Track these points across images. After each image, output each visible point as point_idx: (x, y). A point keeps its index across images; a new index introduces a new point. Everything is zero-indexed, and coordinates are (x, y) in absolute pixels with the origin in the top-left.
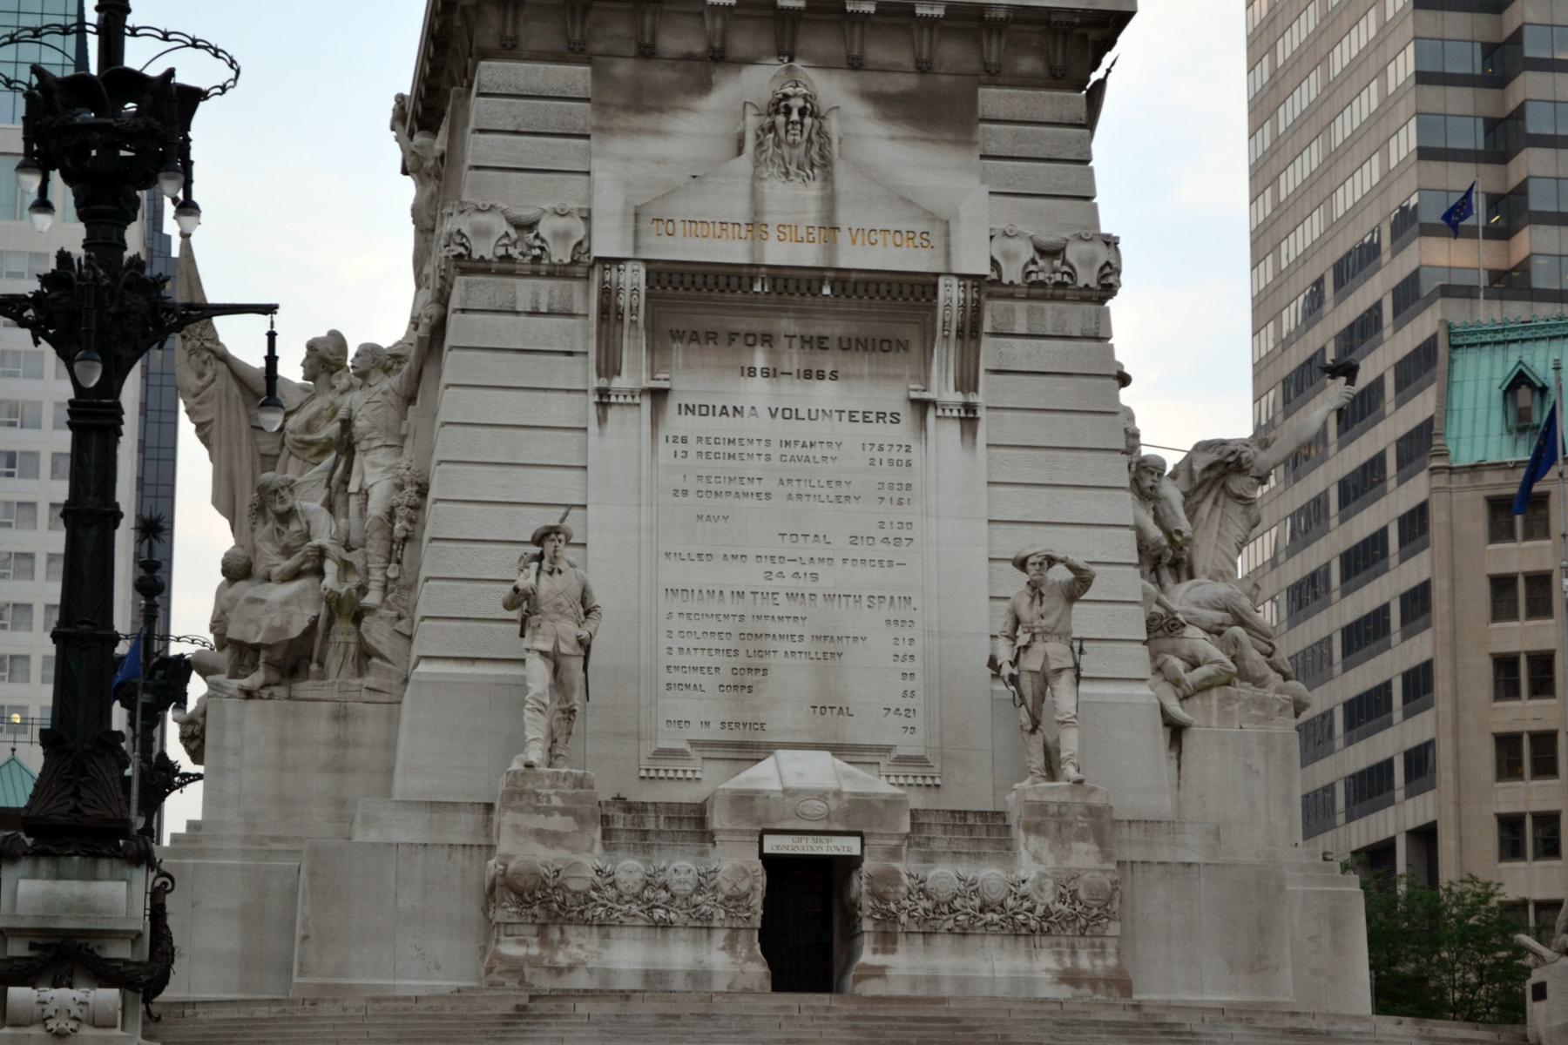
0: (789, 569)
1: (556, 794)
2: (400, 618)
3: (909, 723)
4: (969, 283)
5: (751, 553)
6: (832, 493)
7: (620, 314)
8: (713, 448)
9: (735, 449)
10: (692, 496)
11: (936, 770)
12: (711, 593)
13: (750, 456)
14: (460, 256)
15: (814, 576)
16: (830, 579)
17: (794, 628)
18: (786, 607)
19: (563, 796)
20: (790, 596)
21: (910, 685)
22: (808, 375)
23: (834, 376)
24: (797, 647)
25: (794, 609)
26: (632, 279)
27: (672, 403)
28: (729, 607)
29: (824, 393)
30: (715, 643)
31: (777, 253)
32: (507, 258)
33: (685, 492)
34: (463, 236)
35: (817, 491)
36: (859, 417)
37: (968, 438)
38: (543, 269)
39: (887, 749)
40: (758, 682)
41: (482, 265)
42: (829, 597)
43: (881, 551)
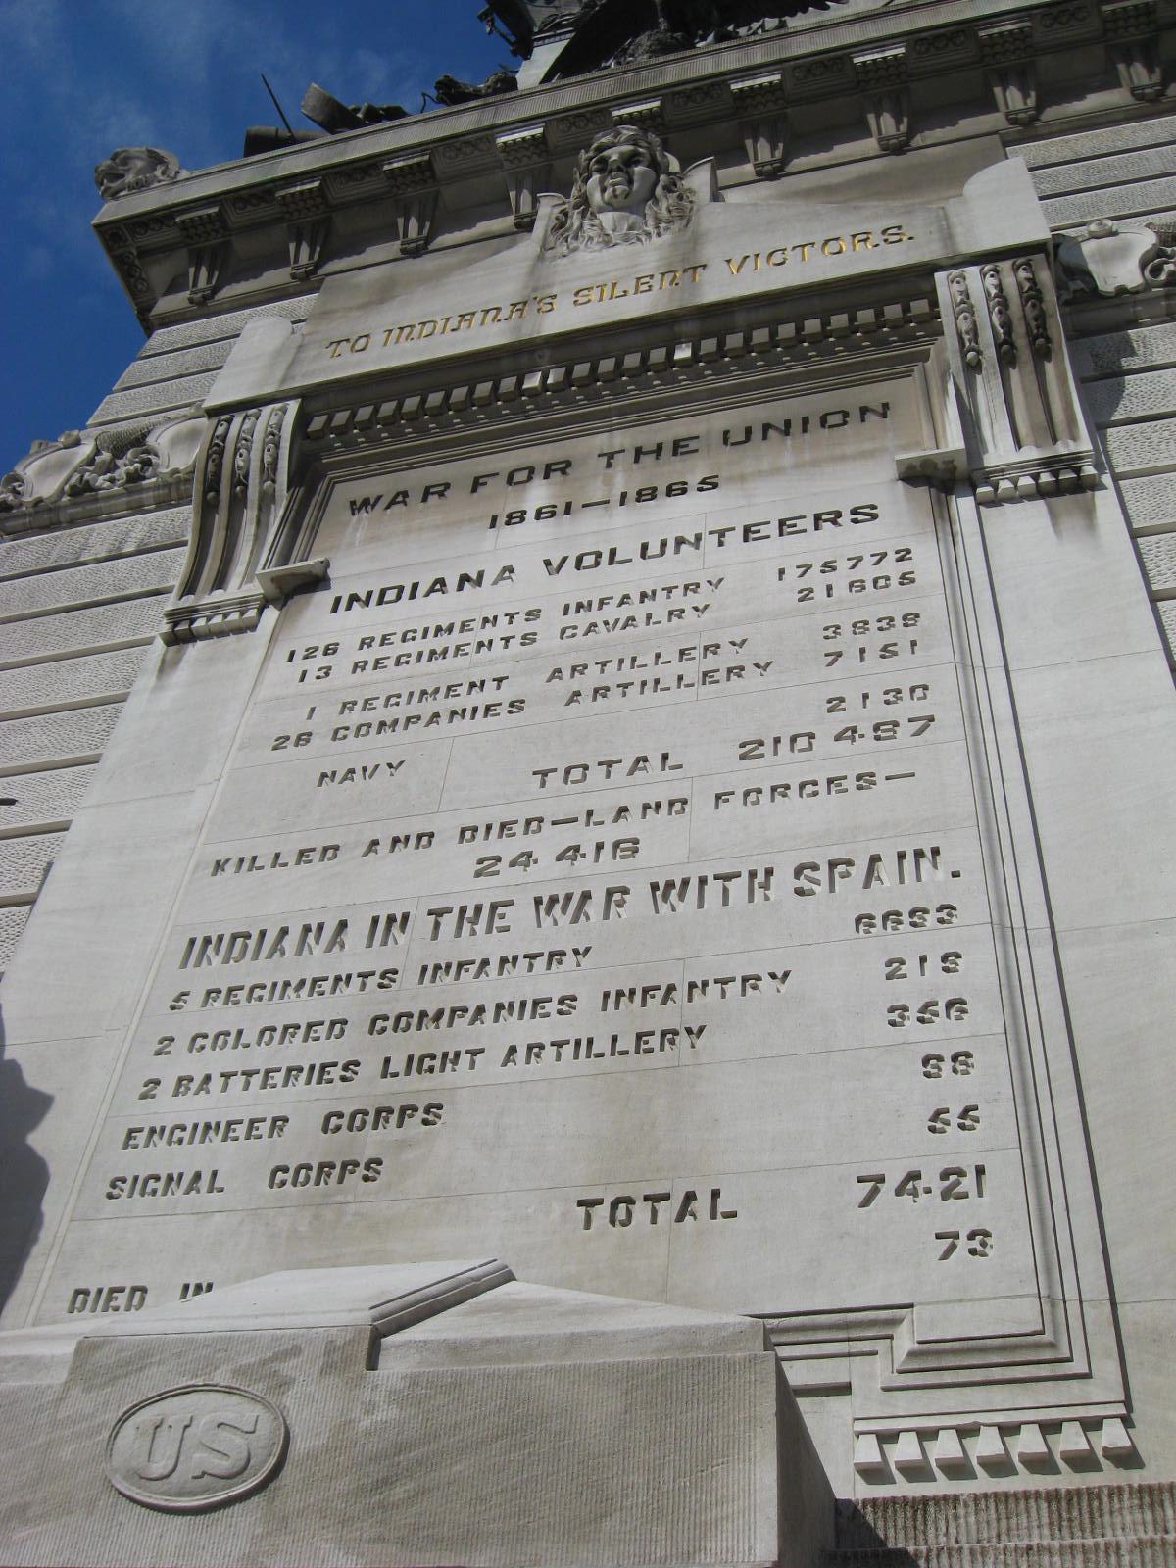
3: (960, 1216)
4: (1005, 266)
6: (691, 670)
11: (1104, 1387)
15: (628, 847)
17: (549, 983)
20: (545, 905)
21: (952, 1091)
23: (709, 484)
24: (541, 1030)
25: (560, 932)
28: (356, 955)
33: (304, 738)
39: (880, 1322)
40: (404, 1144)
42: (663, 891)
43: (832, 758)
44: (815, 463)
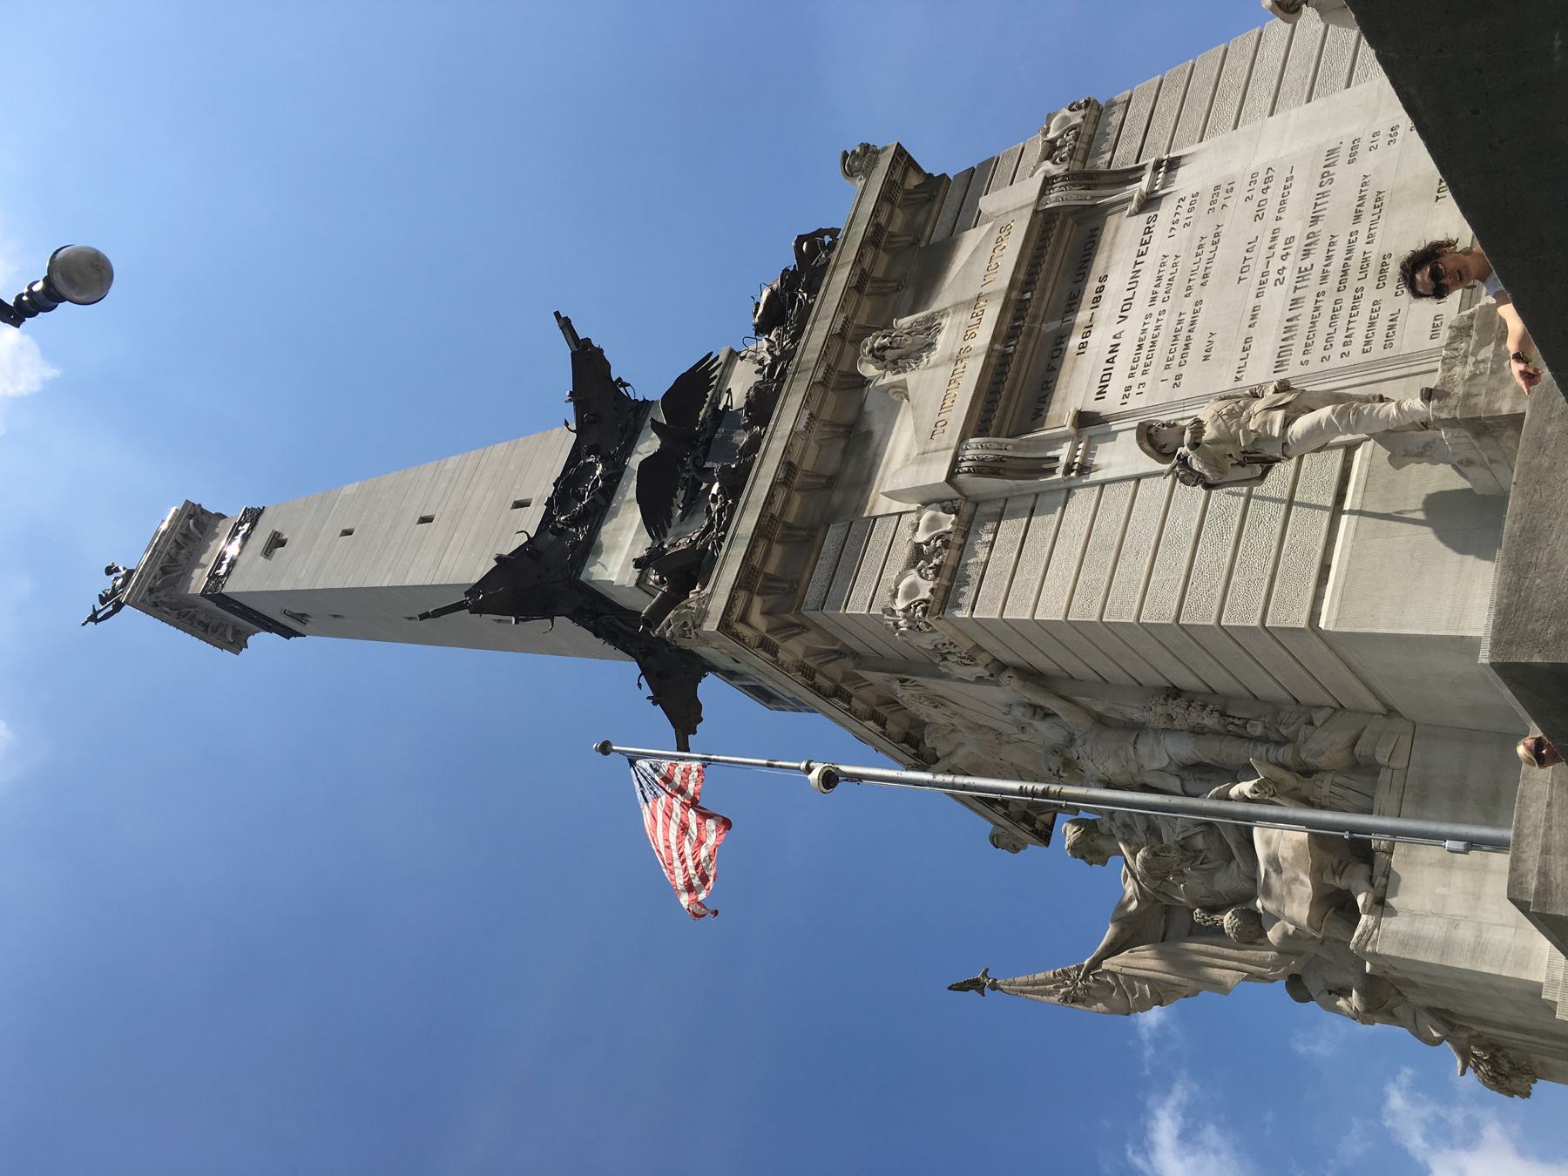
0: (1276, 263)
1: (1474, 354)
2: (1310, 723)
5: (1252, 302)
7: (1001, 460)
8: (1141, 364)
9: (1147, 344)
10: (1183, 370)
12: (1288, 329)
13: (1157, 328)
14: (925, 611)
16: (1294, 225)
18: (1318, 258)
19: (1481, 345)
20: (1307, 254)
22: (1097, 300)
26: (975, 448)
27: (1092, 406)
28: (1307, 309)
29: (1116, 285)
30: (1344, 314)
31: (983, 336)
32: (938, 570)
34: (909, 607)
35: (1204, 261)
36: (1143, 248)
37: (1183, 161)
38: (959, 540)
41: (941, 594)
44: (1112, 244)
